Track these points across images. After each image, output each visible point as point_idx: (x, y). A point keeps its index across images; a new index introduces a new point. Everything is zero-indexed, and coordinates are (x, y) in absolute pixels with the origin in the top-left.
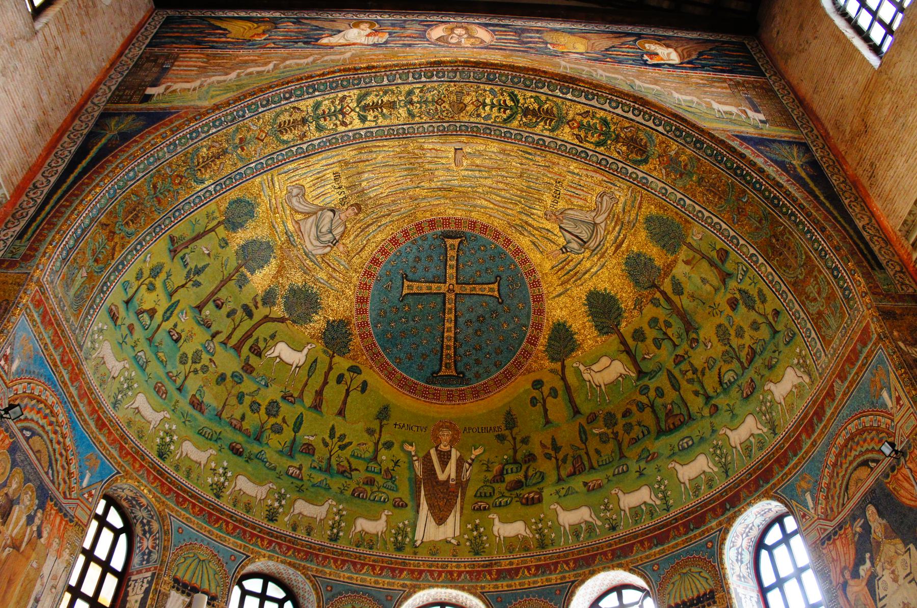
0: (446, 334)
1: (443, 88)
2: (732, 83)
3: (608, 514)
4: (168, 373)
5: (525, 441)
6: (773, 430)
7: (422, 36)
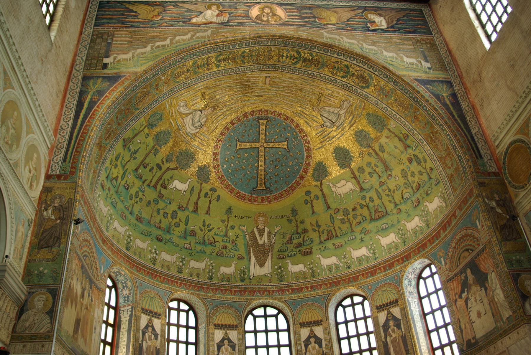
0: (260, 168)
1: (261, 49)
2: (414, 41)
3: (346, 260)
4: (125, 206)
5: (302, 222)
6: (428, 225)
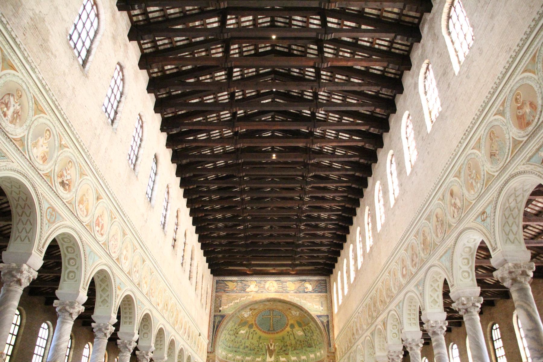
5: (286, 342)
7: (264, 288)
